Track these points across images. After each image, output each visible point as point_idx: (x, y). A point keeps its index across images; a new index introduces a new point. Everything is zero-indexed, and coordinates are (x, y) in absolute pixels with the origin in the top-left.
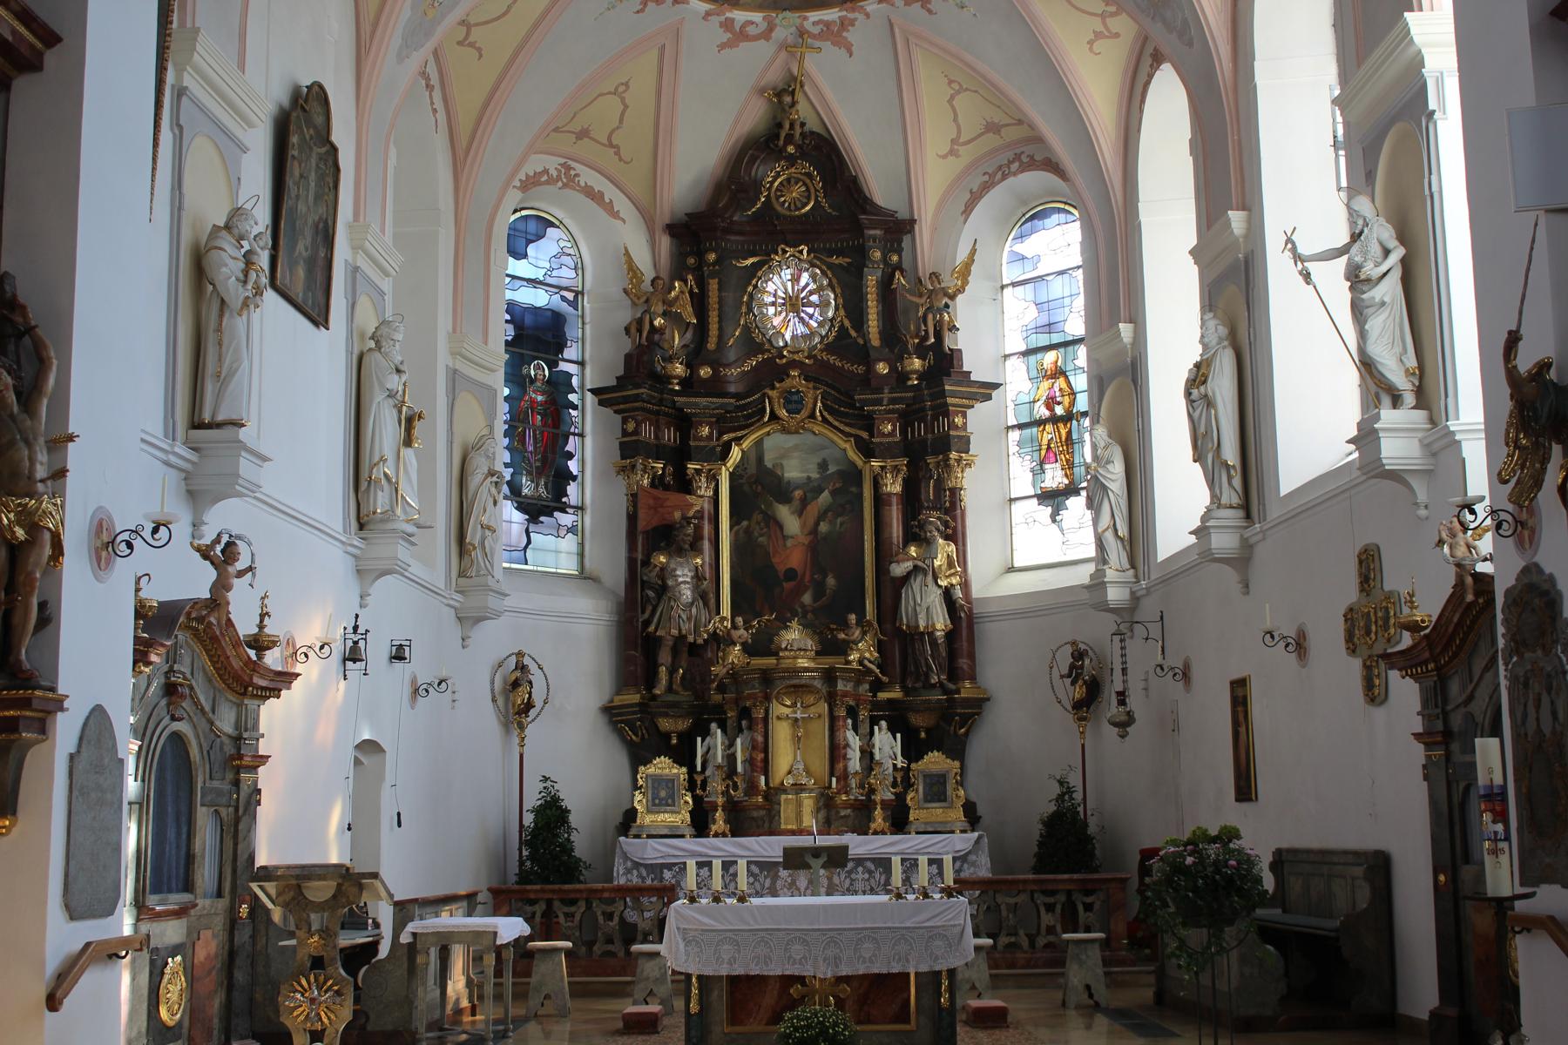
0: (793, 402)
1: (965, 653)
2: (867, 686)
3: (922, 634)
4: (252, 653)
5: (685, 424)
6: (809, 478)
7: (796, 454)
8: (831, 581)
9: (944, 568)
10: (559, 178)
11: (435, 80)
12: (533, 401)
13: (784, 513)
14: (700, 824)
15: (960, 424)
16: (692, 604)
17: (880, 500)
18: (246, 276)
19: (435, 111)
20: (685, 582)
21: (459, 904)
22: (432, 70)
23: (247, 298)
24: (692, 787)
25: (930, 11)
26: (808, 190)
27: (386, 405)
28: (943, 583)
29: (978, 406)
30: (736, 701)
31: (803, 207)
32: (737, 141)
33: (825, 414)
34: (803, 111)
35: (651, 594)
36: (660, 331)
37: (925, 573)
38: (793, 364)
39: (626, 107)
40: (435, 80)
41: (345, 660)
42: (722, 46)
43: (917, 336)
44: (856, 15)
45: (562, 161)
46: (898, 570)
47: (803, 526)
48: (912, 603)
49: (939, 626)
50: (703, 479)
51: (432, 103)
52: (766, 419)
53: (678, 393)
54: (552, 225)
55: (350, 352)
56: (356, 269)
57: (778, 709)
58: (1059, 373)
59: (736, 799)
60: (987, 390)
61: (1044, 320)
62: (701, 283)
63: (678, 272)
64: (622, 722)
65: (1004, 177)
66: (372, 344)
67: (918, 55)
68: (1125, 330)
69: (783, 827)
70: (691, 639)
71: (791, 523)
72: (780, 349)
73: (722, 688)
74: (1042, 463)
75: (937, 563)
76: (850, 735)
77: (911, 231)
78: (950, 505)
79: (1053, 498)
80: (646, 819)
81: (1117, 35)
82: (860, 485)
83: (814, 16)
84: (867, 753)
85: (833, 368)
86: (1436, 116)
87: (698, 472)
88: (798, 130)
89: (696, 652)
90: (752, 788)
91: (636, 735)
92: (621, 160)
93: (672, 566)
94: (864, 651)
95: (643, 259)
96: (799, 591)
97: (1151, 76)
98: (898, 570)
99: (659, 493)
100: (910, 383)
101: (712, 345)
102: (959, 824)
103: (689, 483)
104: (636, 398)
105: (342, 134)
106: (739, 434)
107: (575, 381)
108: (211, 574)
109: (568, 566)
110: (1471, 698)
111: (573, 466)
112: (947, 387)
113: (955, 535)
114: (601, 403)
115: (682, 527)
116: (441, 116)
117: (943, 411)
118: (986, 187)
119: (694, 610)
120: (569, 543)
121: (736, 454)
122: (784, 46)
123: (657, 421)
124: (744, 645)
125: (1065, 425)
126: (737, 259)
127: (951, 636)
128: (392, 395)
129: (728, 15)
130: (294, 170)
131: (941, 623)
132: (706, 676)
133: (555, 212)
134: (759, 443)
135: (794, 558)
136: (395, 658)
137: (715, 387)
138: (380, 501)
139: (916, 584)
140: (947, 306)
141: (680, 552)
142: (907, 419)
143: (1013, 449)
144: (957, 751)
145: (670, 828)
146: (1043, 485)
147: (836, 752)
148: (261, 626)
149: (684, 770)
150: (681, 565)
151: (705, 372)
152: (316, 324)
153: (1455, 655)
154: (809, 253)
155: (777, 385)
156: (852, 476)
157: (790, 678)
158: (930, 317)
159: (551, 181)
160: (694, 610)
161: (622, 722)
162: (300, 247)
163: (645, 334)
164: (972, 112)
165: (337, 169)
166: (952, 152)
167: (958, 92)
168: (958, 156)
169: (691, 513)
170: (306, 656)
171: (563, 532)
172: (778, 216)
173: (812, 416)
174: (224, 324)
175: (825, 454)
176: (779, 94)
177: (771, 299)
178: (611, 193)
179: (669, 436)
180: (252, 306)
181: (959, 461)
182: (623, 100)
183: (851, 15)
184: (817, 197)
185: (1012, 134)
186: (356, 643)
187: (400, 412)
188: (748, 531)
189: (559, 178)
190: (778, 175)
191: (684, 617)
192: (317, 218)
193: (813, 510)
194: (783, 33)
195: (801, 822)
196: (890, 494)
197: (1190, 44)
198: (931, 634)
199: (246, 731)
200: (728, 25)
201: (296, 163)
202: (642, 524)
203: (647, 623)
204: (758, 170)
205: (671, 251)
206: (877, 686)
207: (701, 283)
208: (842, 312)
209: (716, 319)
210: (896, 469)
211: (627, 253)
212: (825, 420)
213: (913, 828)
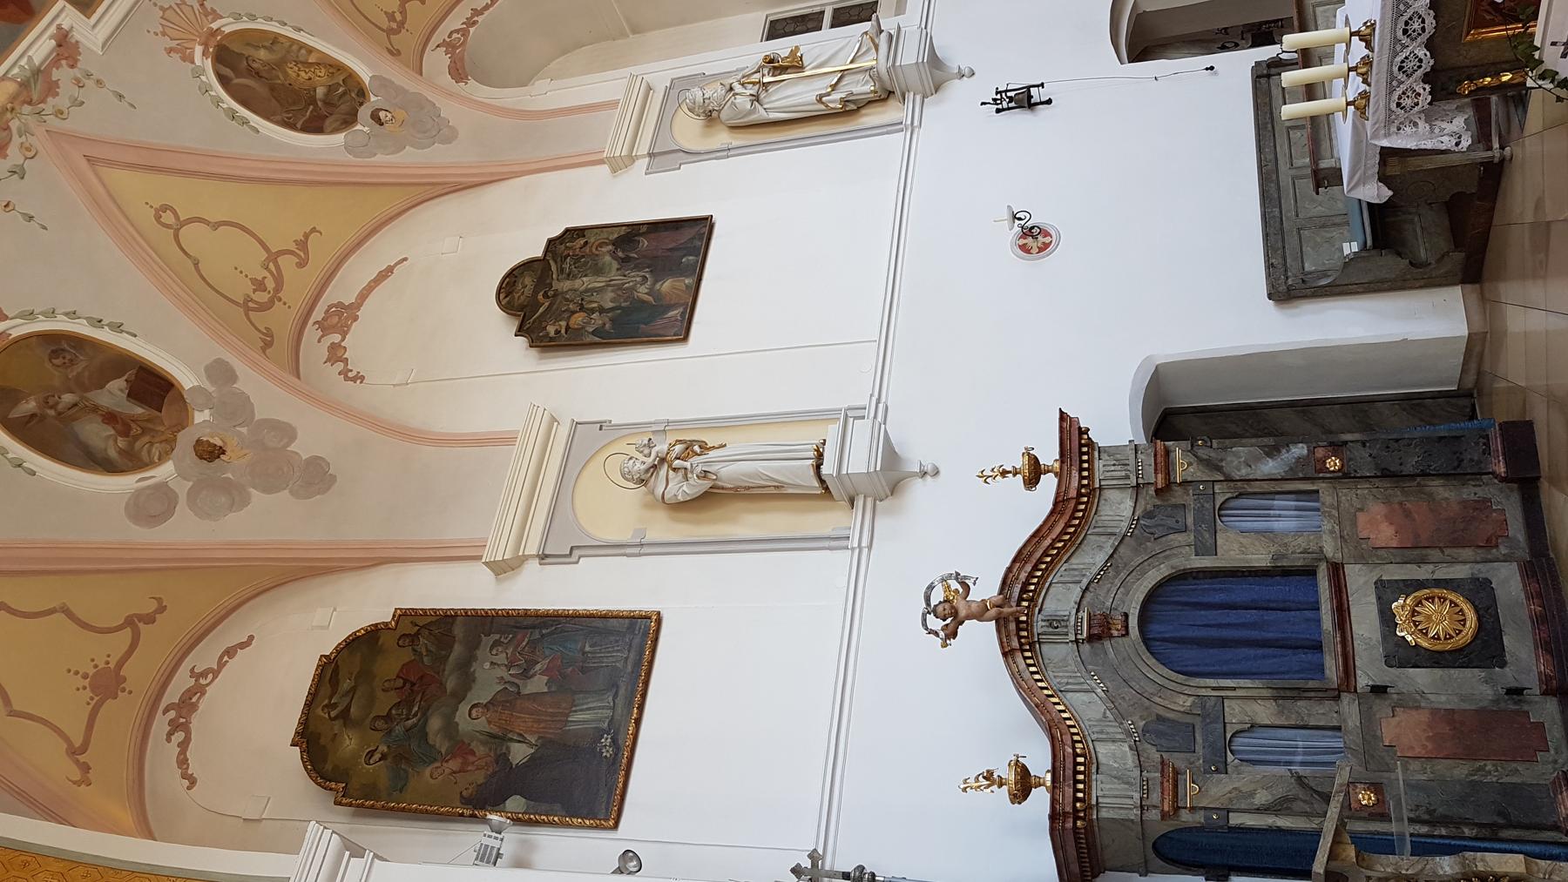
27: (766, 100)
55: (727, 152)
56: (651, 155)
128: (756, 98)
138: (862, 87)
152: (712, 227)
165: (567, 230)
174: (730, 486)
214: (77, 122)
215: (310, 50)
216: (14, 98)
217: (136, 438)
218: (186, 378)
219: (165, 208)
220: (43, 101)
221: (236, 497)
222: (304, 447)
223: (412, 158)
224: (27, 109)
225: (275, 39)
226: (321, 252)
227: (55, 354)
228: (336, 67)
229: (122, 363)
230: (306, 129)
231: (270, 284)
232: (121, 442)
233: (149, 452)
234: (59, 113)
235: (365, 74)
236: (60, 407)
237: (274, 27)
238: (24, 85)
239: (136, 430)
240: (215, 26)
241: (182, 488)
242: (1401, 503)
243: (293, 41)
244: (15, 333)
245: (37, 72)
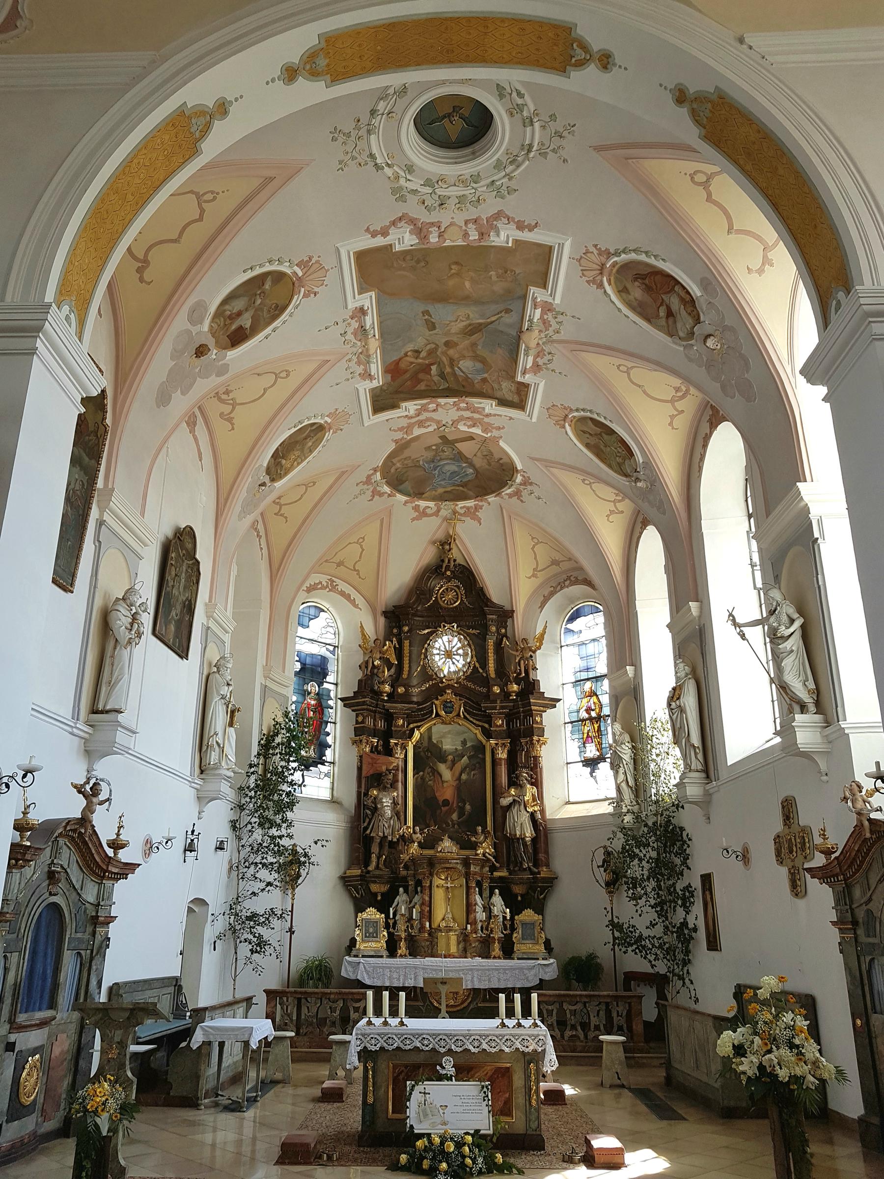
0: (448, 707)
1: (543, 851)
2: (487, 869)
3: (518, 839)
4: (110, 852)
5: (389, 718)
6: (456, 749)
7: (449, 736)
8: (468, 807)
9: (530, 801)
10: (327, 586)
11: (262, 533)
12: (309, 704)
13: (442, 768)
14: (392, 949)
15: (539, 721)
16: (391, 818)
17: (495, 762)
18: (132, 626)
19: (261, 549)
20: (387, 806)
21: (241, 1005)
22: (261, 527)
23: (131, 638)
24: (387, 926)
25: (522, 501)
26: (457, 594)
28: (530, 810)
29: (548, 711)
30: (414, 875)
31: (455, 603)
32: (421, 568)
33: (466, 714)
34: (455, 554)
35: (369, 812)
36: (378, 667)
37: (519, 803)
38: (449, 686)
39: (363, 550)
40: (262, 533)
41: (185, 850)
42: (413, 520)
43: (515, 672)
44: (483, 503)
45: (330, 577)
46: (505, 802)
47: (453, 775)
48: (512, 821)
49: (527, 835)
50: (399, 749)
51: (260, 545)
52: (434, 716)
53: (386, 701)
54: (323, 611)
56: (208, 628)
57: (437, 881)
58: (592, 694)
59: (413, 934)
60: (553, 702)
61: (583, 664)
62: (400, 642)
63: (388, 637)
64: (350, 885)
65: (561, 589)
66: (215, 669)
67: (516, 525)
68: (630, 669)
69: (439, 952)
70: (390, 838)
71: (447, 774)
72: (441, 679)
73: (406, 867)
74: (584, 743)
75: (526, 798)
76: (478, 898)
77: (512, 617)
78: (534, 766)
79: (591, 763)
80: (361, 946)
81: (622, 512)
82: (484, 753)
83: (461, 504)
84: (488, 909)
85: (470, 689)
86: (819, 541)
87: (396, 744)
88: (452, 563)
89: (393, 846)
90: (422, 929)
91: (359, 894)
92: (360, 577)
93: (380, 796)
94: (486, 849)
95: (370, 630)
96: (450, 812)
97: (641, 533)
98: (505, 802)
99: (375, 756)
100: (511, 698)
101: (405, 676)
102: (542, 954)
103: (392, 749)
104: (364, 703)
105: (204, 554)
106: (419, 724)
107: (332, 694)
108: (82, 802)
109: (326, 795)
110: (870, 900)
111: (329, 739)
112: (531, 700)
113: (537, 782)
114: (345, 706)
115: (386, 774)
116: (265, 551)
117: (530, 714)
118: (552, 594)
119: (392, 822)
120: (327, 782)
121: (417, 735)
122: (446, 519)
123: (375, 716)
124: (419, 843)
125: (597, 723)
126: (420, 630)
127: (534, 840)
128: (223, 697)
129: (416, 503)
130: (171, 572)
131: (529, 833)
132: (397, 860)
133: (325, 604)
134: (430, 729)
135: (447, 793)
136: (218, 848)
137: (406, 698)
138: (214, 757)
139: (515, 810)
140: (531, 656)
141: (385, 789)
142: (510, 718)
143: (568, 734)
144: (540, 910)
145: (375, 951)
146: (585, 755)
147: (470, 908)
148: (118, 835)
149: (383, 915)
150: (385, 796)
151: (401, 690)
152: (181, 657)
153: (857, 871)
154: (457, 628)
155: (440, 698)
156: (480, 749)
157: (444, 863)
158: (522, 662)
159: (324, 588)
160: (392, 822)
161: (350, 885)
162: (173, 613)
163: (369, 669)
164: (544, 554)
165: (200, 574)
166: (534, 575)
167: (537, 544)
168: (537, 577)
169: (391, 768)
170: (158, 848)
171: (322, 776)
172: (441, 608)
173: (458, 715)
175: (465, 736)
176: (442, 544)
177: (438, 652)
178: (354, 594)
179: (381, 724)
180: (134, 643)
181: (538, 741)
182: (361, 546)
183: (480, 504)
184: (462, 598)
185: (566, 566)
186: (192, 840)
187: (228, 707)
188: (422, 778)
189: (327, 586)
190: (442, 587)
191: (386, 826)
192: (184, 599)
193: (458, 767)
194: (444, 513)
195: (449, 950)
196: (501, 759)
197: (664, 514)
198: (523, 839)
199: (103, 900)
200: (417, 508)
201: (173, 568)
202: (364, 774)
203: (366, 829)
204: (432, 583)
205: (385, 625)
206: (493, 869)
207: (400, 642)
208: (475, 659)
209: (408, 662)
210: (504, 745)
211: (362, 627)
212: (465, 717)
213: (515, 956)
214: (343, 364)
215: (299, 464)
216: (367, 350)
217: (225, 321)
218: (232, 354)
219: (288, 376)
220: (358, 358)
221: (176, 354)
222: (177, 396)
223: (242, 494)
224: (360, 351)
225: (311, 452)
226: (221, 426)
227: (277, 306)
228: (286, 474)
229: (255, 329)
230: (277, 449)
231: (224, 397)
232: (228, 313)
233: (217, 323)
234: (350, 360)
235: (277, 484)
236: (258, 296)
237: (315, 453)
238: (369, 356)
239: (228, 322)
240: (331, 431)
241: (194, 330)
242: (66, 1059)
243: (306, 458)
244: (296, 297)
245: (369, 362)
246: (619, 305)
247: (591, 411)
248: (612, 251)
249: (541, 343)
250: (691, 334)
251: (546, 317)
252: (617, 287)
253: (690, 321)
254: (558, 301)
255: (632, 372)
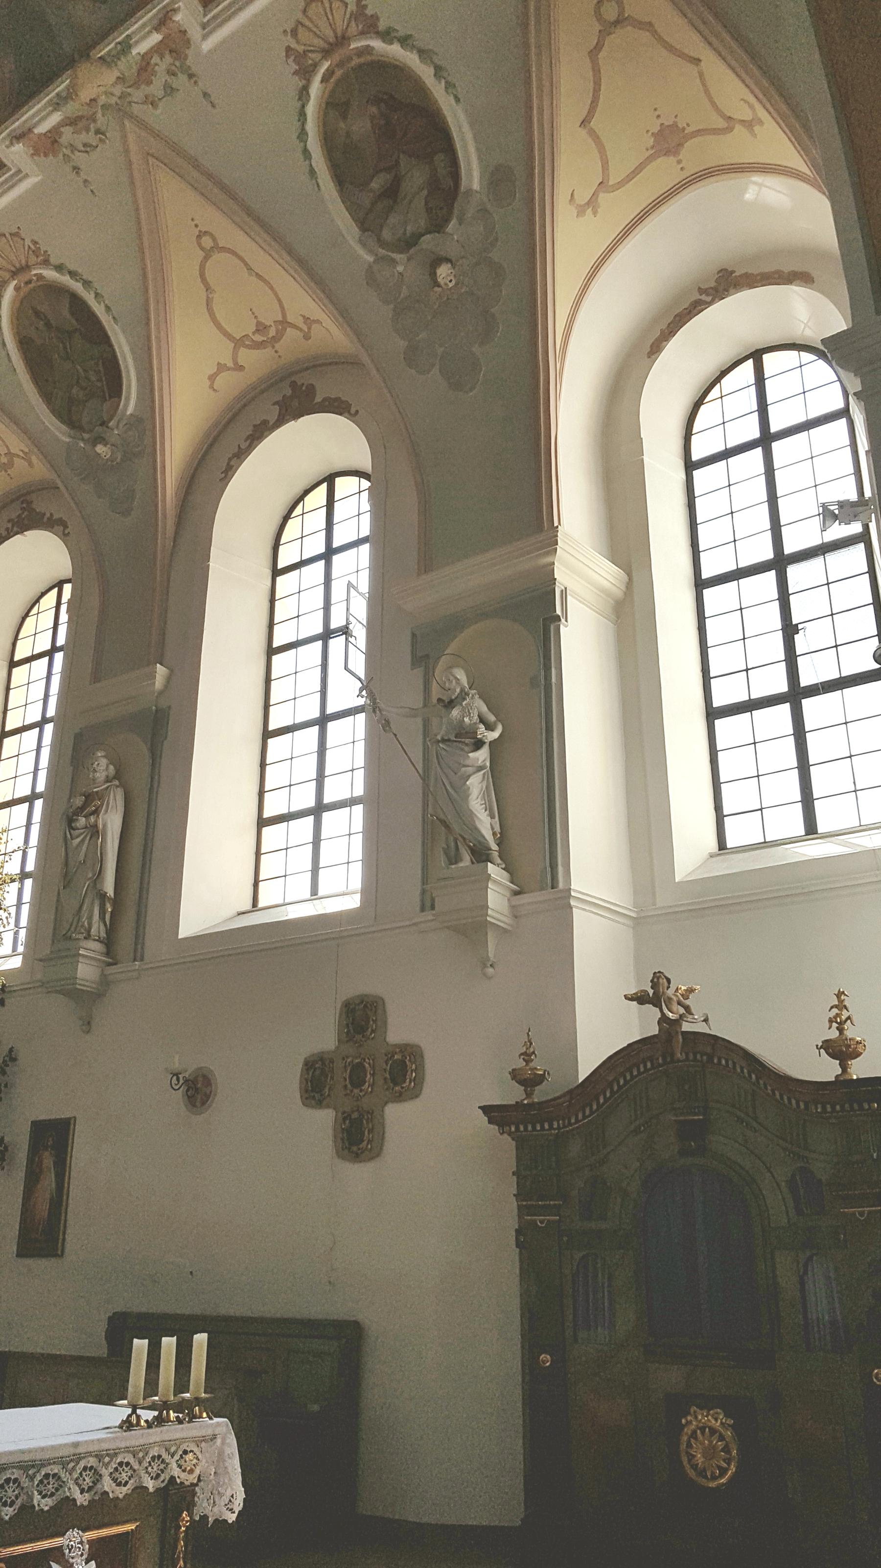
246: (311, 126)
247: (87, 284)
248: (382, 25)
249: (101, 103)
250: (408, 243)
251: (156, 59)
252: (333, 91)
253: (418, 220)
254: (207, 46)
255: (217, 257)
